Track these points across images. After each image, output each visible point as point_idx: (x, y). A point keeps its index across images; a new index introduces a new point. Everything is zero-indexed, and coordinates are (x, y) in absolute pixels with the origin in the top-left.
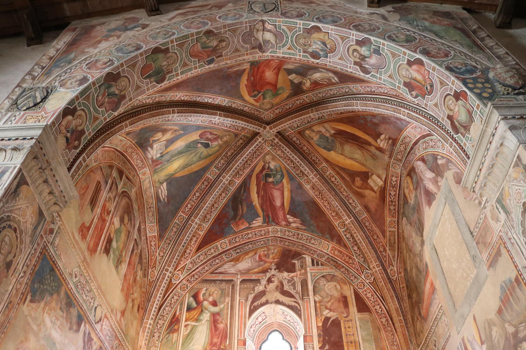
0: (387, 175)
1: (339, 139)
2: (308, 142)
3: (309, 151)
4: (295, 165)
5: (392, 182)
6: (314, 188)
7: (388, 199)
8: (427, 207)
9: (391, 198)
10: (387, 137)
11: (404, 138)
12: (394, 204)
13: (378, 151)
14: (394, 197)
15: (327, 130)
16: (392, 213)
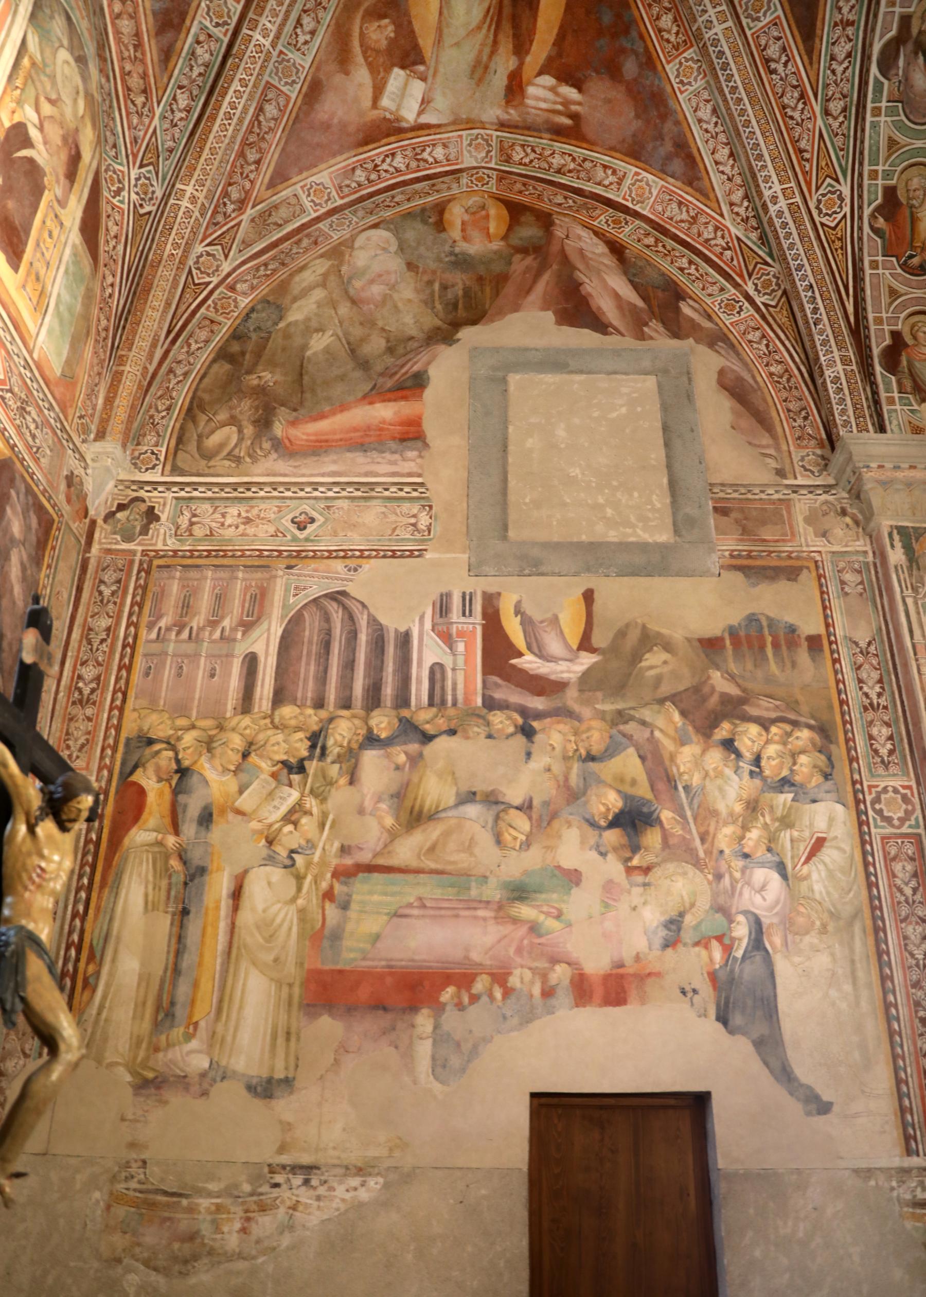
0: (439, 126)
5: (428, 150)
7: (376, 152)
8: (550, 316)
9: (383, 161)
10: (574, 108)
11: (605, 167)
12: (373, 176)
13: (505, 82)
14: (392, 170)
16: (347, 182)
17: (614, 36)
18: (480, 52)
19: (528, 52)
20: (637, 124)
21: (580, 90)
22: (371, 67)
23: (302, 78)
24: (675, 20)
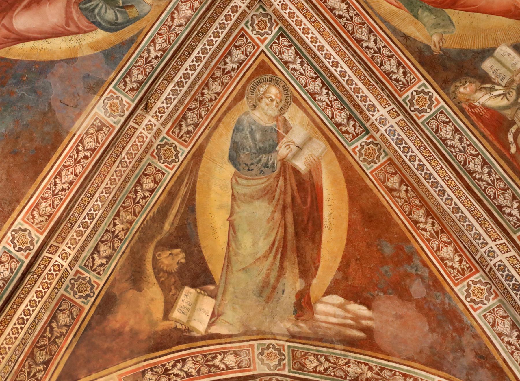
1: (281, 182)
2: (240, 96)
3: (211, 100)
4: (155, 62)
6: (100, 129)
13: (294, 300)
15: (300, 148)
17: (398, 263)
18: (268, 275)
19: (314, 276)
20: (432, 338)
21: (369, 307)
22: (162, 285)
23: (96, 293)
24: (456, 251)
